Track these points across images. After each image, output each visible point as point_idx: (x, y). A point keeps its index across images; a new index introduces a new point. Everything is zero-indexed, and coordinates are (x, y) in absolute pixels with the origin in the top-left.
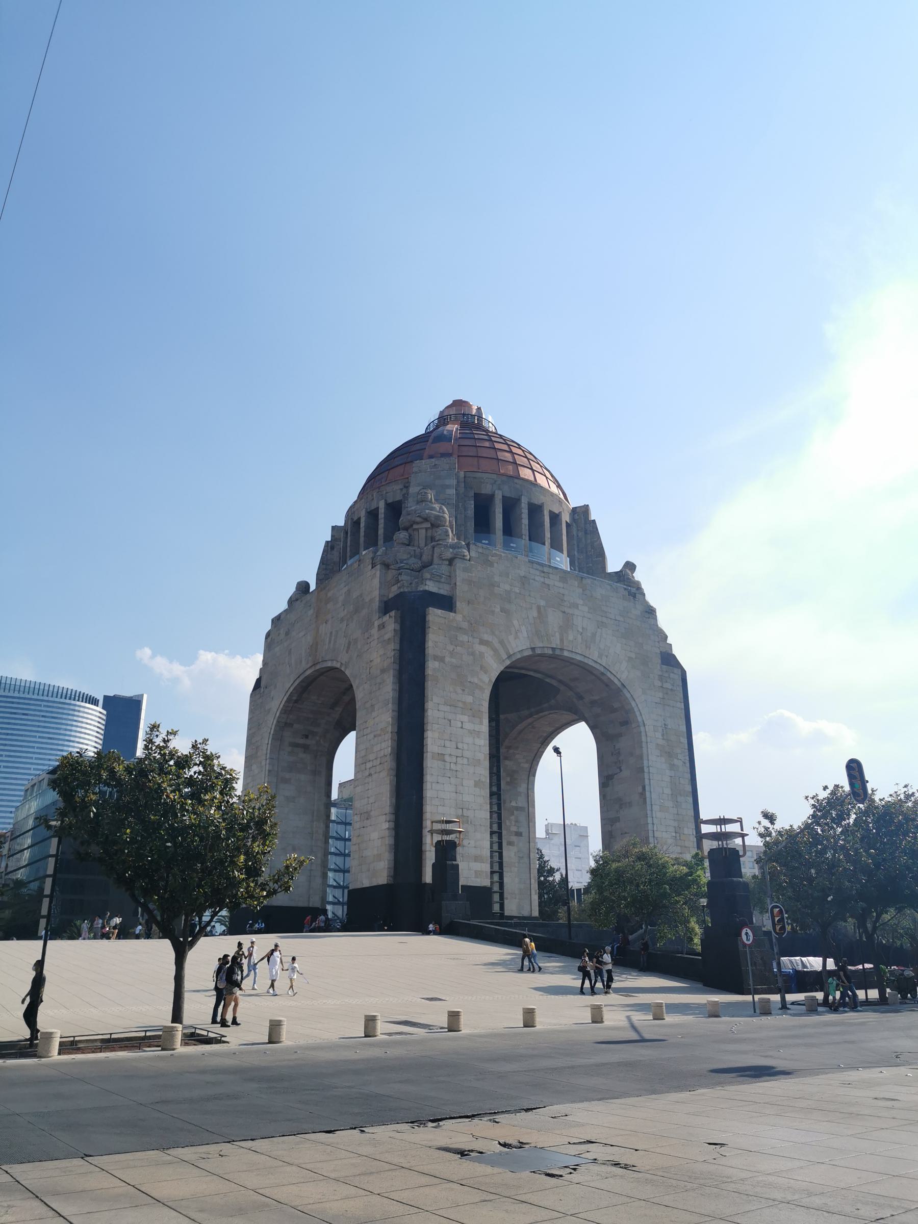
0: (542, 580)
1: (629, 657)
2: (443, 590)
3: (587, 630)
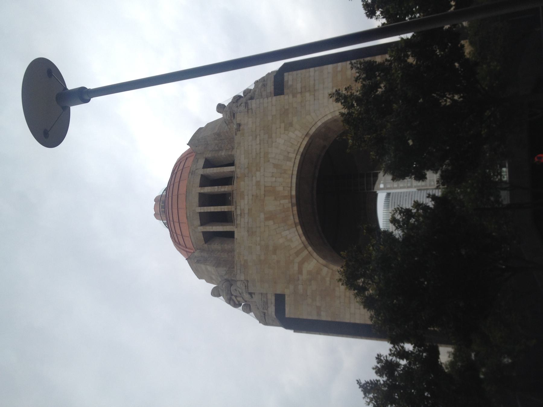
0: (246, 216)
1: (285, 130)
2: (272, 299)
3: (273, 173)
